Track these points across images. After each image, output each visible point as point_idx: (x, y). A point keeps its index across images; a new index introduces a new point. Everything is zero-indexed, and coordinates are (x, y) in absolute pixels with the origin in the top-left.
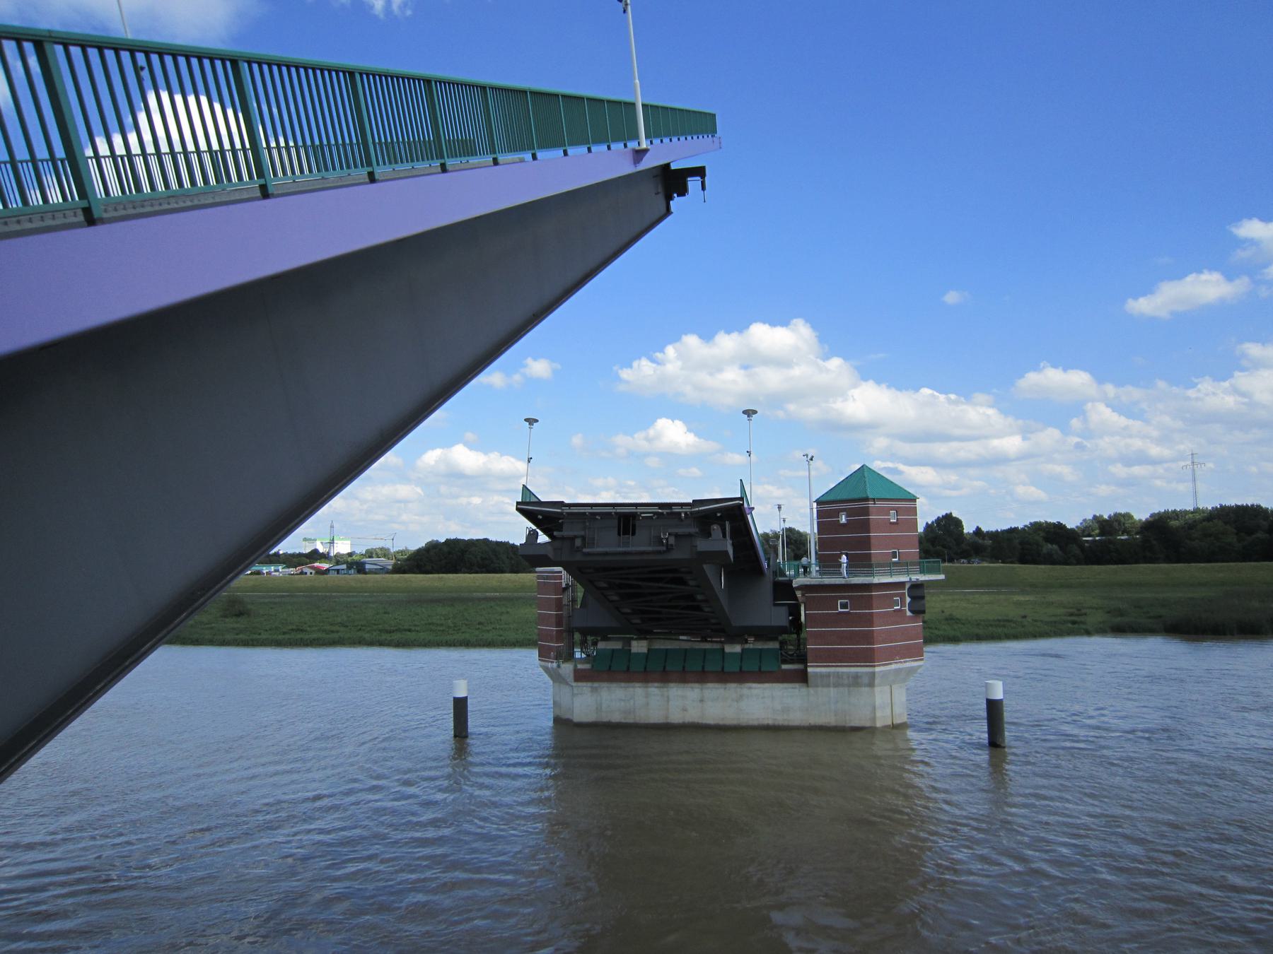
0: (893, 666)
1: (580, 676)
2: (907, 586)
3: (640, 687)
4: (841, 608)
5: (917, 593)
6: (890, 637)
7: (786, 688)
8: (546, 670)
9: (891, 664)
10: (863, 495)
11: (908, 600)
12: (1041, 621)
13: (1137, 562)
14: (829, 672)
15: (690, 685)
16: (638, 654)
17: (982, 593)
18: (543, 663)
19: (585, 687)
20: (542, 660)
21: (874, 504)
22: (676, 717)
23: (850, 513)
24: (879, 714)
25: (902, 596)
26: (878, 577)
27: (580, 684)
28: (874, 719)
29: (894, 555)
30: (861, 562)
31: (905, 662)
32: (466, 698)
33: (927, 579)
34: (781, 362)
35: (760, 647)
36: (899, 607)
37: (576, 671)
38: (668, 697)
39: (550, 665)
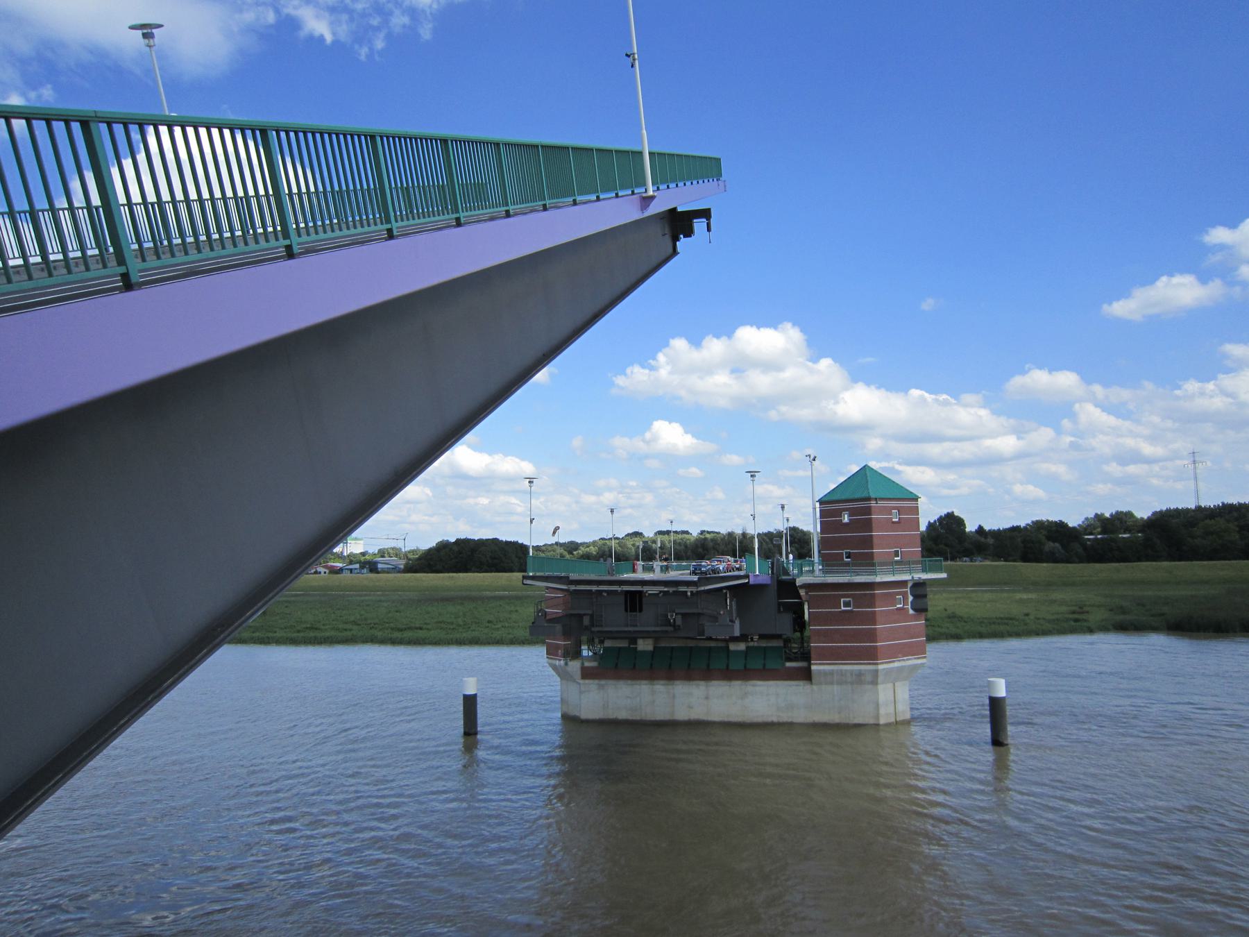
0: (896, 664)
1: (587, 674)
2: (910, 585)
3: (646, 684)
5: (919, 591)
7: (790, 686)
8: (555, 668)
9: (894, 662)
10: (865, 495)
11: (911, 598)
12: (1044, 619)
13: (1139, 560)
14: (833, 670)
16: (644, 652)
17: (986, 591)
18: (550, 661)
19: (592, 684)
20: (551, 658)
21: (877, 503)
22: (682, 714)
23: (852, 512)
24: (882, 711)
25: (905, 595)
27: (587, 681)
28: (877, 717)
29: (896, 554)
30: (866, 561)
31: (907, 660)
32: (476, 695)
35: (764, 645)
36: (901, 606)
37: (583, 669)
39: (557, 663)
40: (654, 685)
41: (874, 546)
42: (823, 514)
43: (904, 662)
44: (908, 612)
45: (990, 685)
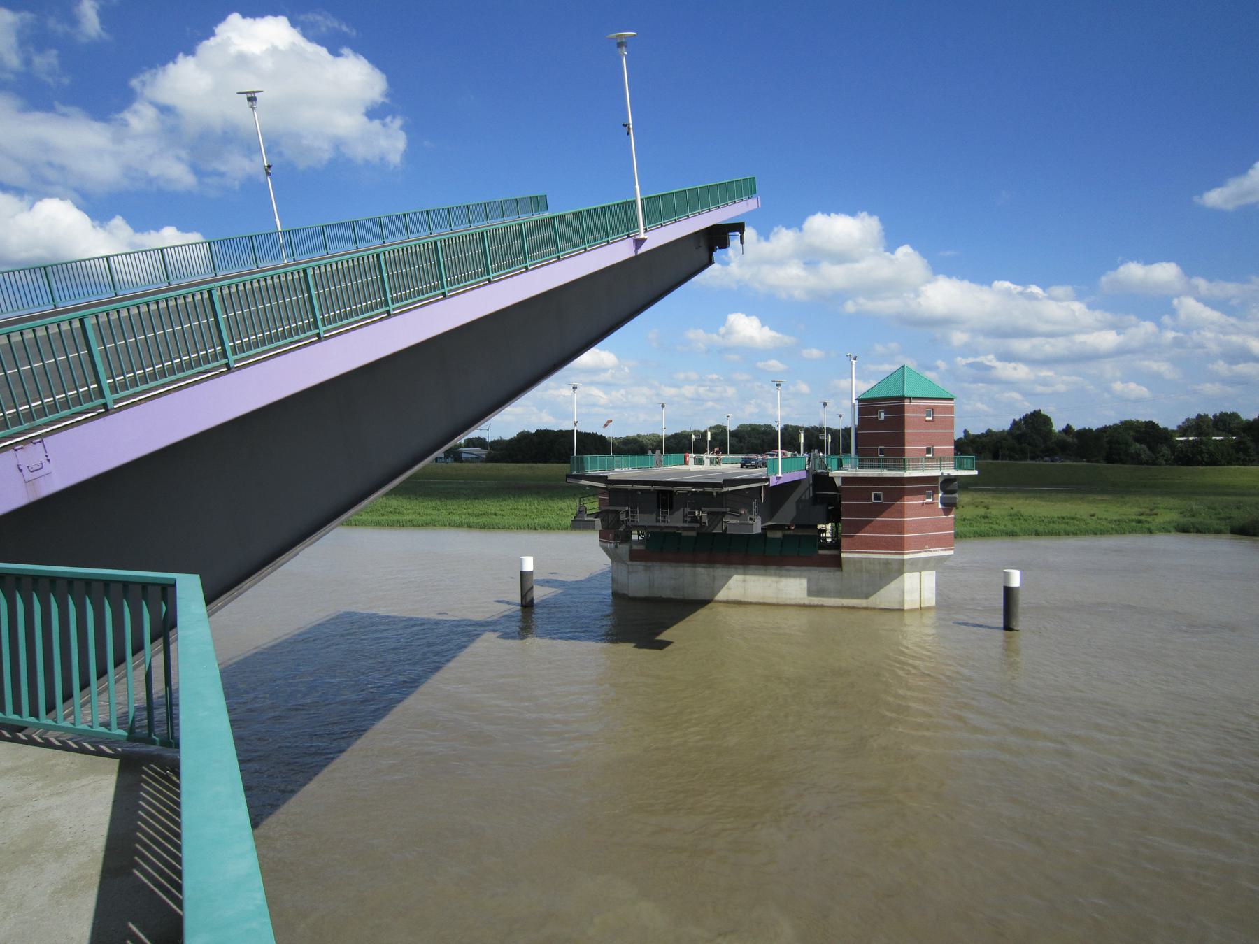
0: (923, 555)
1: (635, 556)
2: (940, 480)
3: (689, 567)
4: (875, 499)
6: (920, 527)
8: (606, 550)
9: (920, 552)
10: (900, 394)
12: (1106, 519)
13: (1229, 463)
18: (603, 544)
19: (639, 566)
20: (603, 541)
24: (907, 597)
26: (910, 471)
27: (635, 563)
28: (902, 602)
29: (928, 451)
30: (897, 455)
31: (934, 551)
33: (959, 474)
35: (800, 534)
36: (930, 500)
37: (632, 552)
38: (714, 577)
39: (608, 545)
40: (695, 567)
41: (906, 443)
42: (861, 411)
43: (930, 553)
44: (938, 506)
45: (1007, 576)
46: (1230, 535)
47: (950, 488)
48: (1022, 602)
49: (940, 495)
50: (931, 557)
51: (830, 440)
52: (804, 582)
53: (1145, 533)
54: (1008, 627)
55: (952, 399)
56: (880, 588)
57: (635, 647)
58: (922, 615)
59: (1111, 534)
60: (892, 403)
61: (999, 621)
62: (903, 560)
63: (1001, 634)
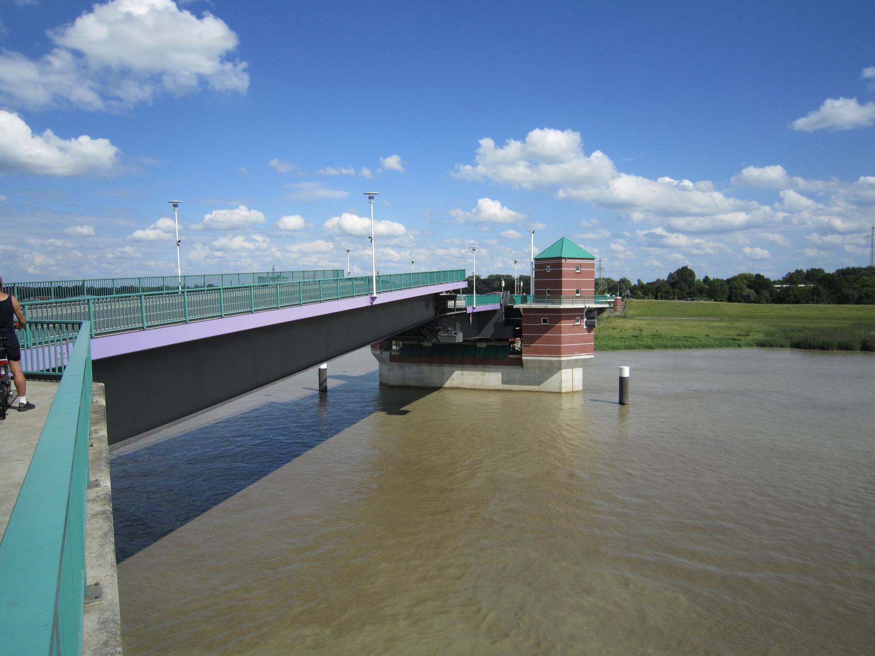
0: (573, 358)
1: (393, 359)
2: (585, 311)
4: (543, 323)
6: (571, 340)
8: (375, 355)
10: (558, 255)
12: (713, 338)
13: (807, 302)
15: (456, 365)
17: (693, 321)
18: (373, 351)
19: (396, 365)
23: (553, 266)
24: (564, 385)
27: (393, 364)
28: (561, 388)
29: (577, 292)
30: (556, 294)
31: (581, 355)
34: (552, 160)
35: (497, 345)
36: (579, 323)
37: (391, 356)
39: (376, 352)
42: (537, 266)
45: (621, 370)
46: (790, 348)
47: (591, 315)
48: (631, 386)
49: (585, 320)
50: (579, 359)
51: (522, 285)
52: (499, 375)
53: (736, 347)
54: (622, 403)
55: (593, 259)
56: (547, 379)
57: (387, 414)
58: (573, 396)
59: (714, 347)
60: (556, 261)
61: (616, 398)
62: (561, 361)
63: (618, 406)
